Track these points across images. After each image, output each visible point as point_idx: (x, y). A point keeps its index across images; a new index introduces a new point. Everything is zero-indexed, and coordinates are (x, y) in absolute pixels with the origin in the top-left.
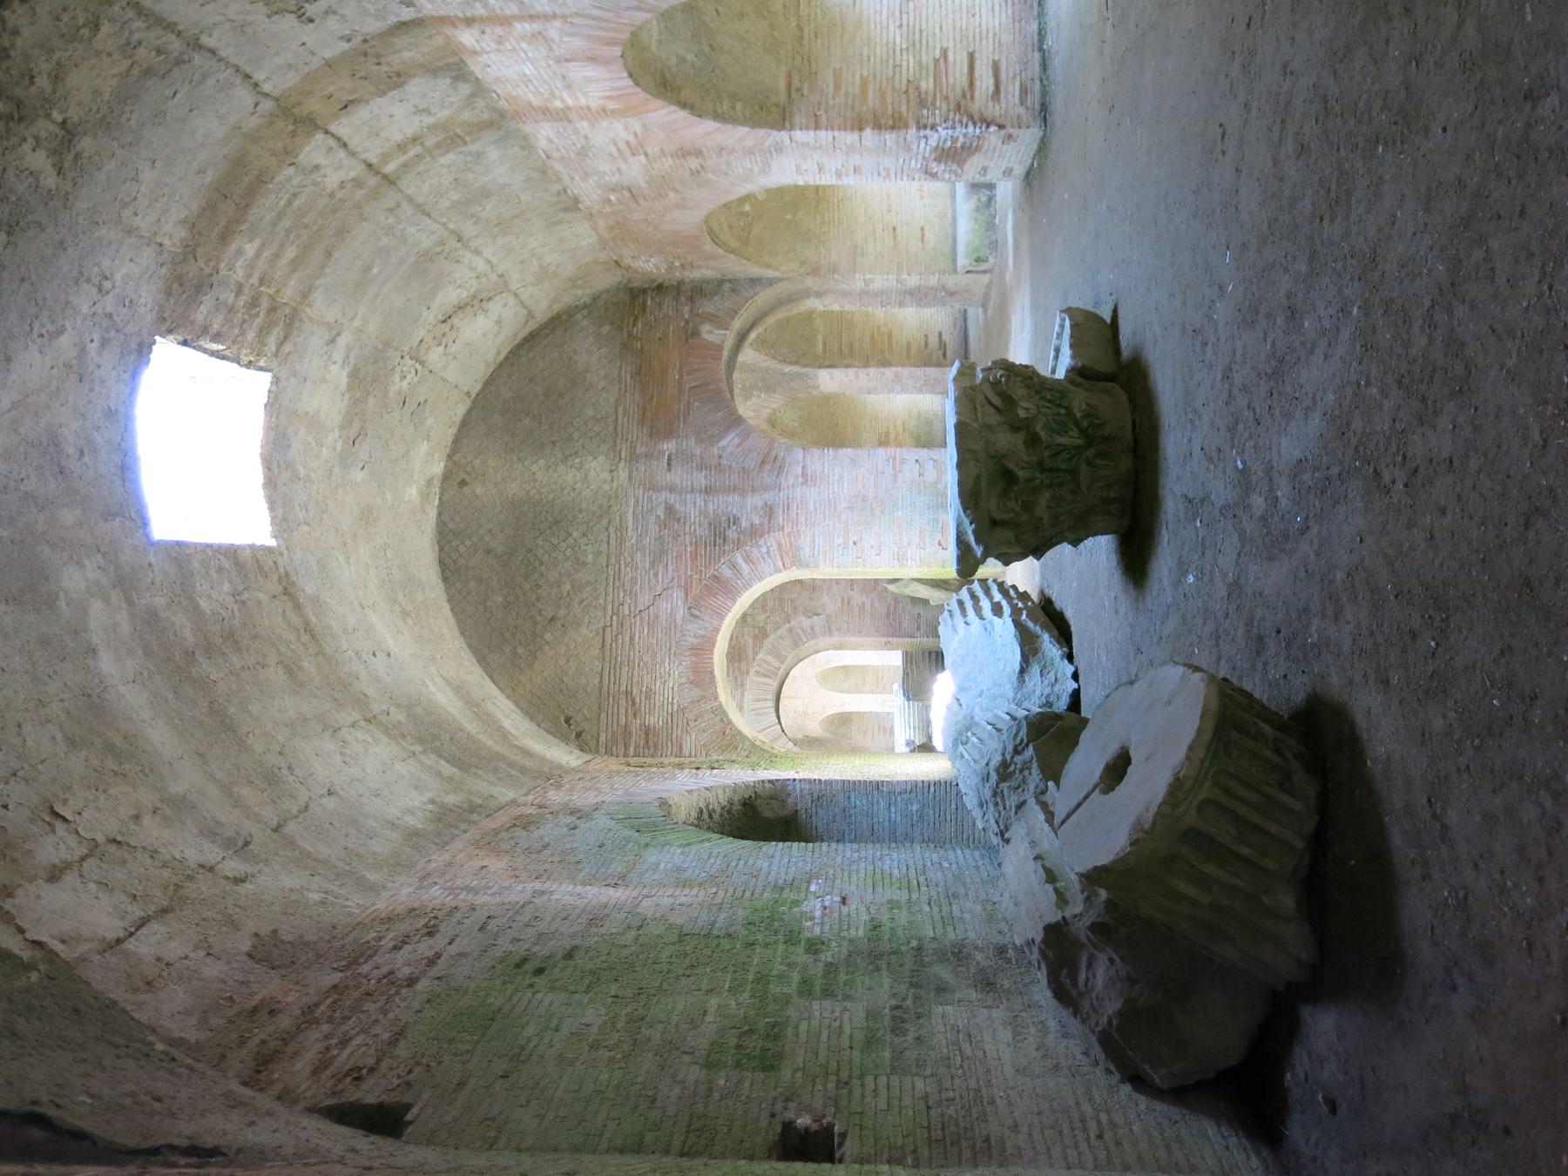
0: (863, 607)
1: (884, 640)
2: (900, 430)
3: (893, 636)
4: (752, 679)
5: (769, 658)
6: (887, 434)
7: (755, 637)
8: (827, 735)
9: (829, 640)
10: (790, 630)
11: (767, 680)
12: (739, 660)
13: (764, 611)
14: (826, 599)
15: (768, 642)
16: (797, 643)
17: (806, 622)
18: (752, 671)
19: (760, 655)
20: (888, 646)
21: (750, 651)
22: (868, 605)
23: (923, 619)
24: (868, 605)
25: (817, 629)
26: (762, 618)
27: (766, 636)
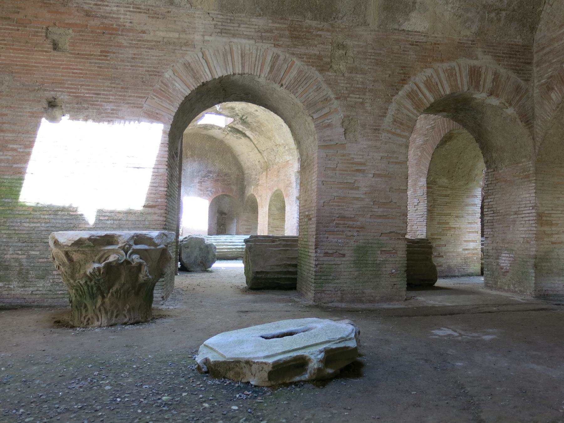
0: (353, 187)
1: (314, 212)
2: (555, 238)
3: (318, 223)
4: (269, 51)
5: (294, 73)
6: (550, 224)
7: (320, 58)
8: (246, 199)
9: (314, 153)
10: (326, 100)
11: (267, 69)
12: (293, 37)
13: (352, 70)
14: (363, 143)
15: (313, 72)
16: (311, 106)
17: (336, 119)
18: (275, 50)
19: (298, 63)
20: (304, 218)
21: (303, 50)
22: (354, 194)
23: (338, 260)
24: (354, 194)
25: (328, 132)
26: (342, 68)
27: (321, 70)
